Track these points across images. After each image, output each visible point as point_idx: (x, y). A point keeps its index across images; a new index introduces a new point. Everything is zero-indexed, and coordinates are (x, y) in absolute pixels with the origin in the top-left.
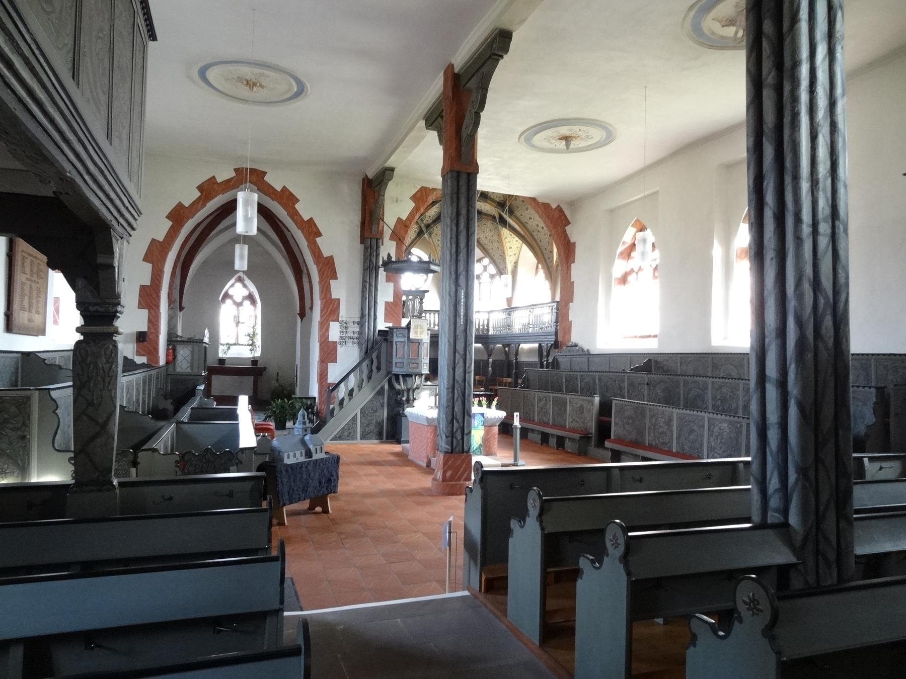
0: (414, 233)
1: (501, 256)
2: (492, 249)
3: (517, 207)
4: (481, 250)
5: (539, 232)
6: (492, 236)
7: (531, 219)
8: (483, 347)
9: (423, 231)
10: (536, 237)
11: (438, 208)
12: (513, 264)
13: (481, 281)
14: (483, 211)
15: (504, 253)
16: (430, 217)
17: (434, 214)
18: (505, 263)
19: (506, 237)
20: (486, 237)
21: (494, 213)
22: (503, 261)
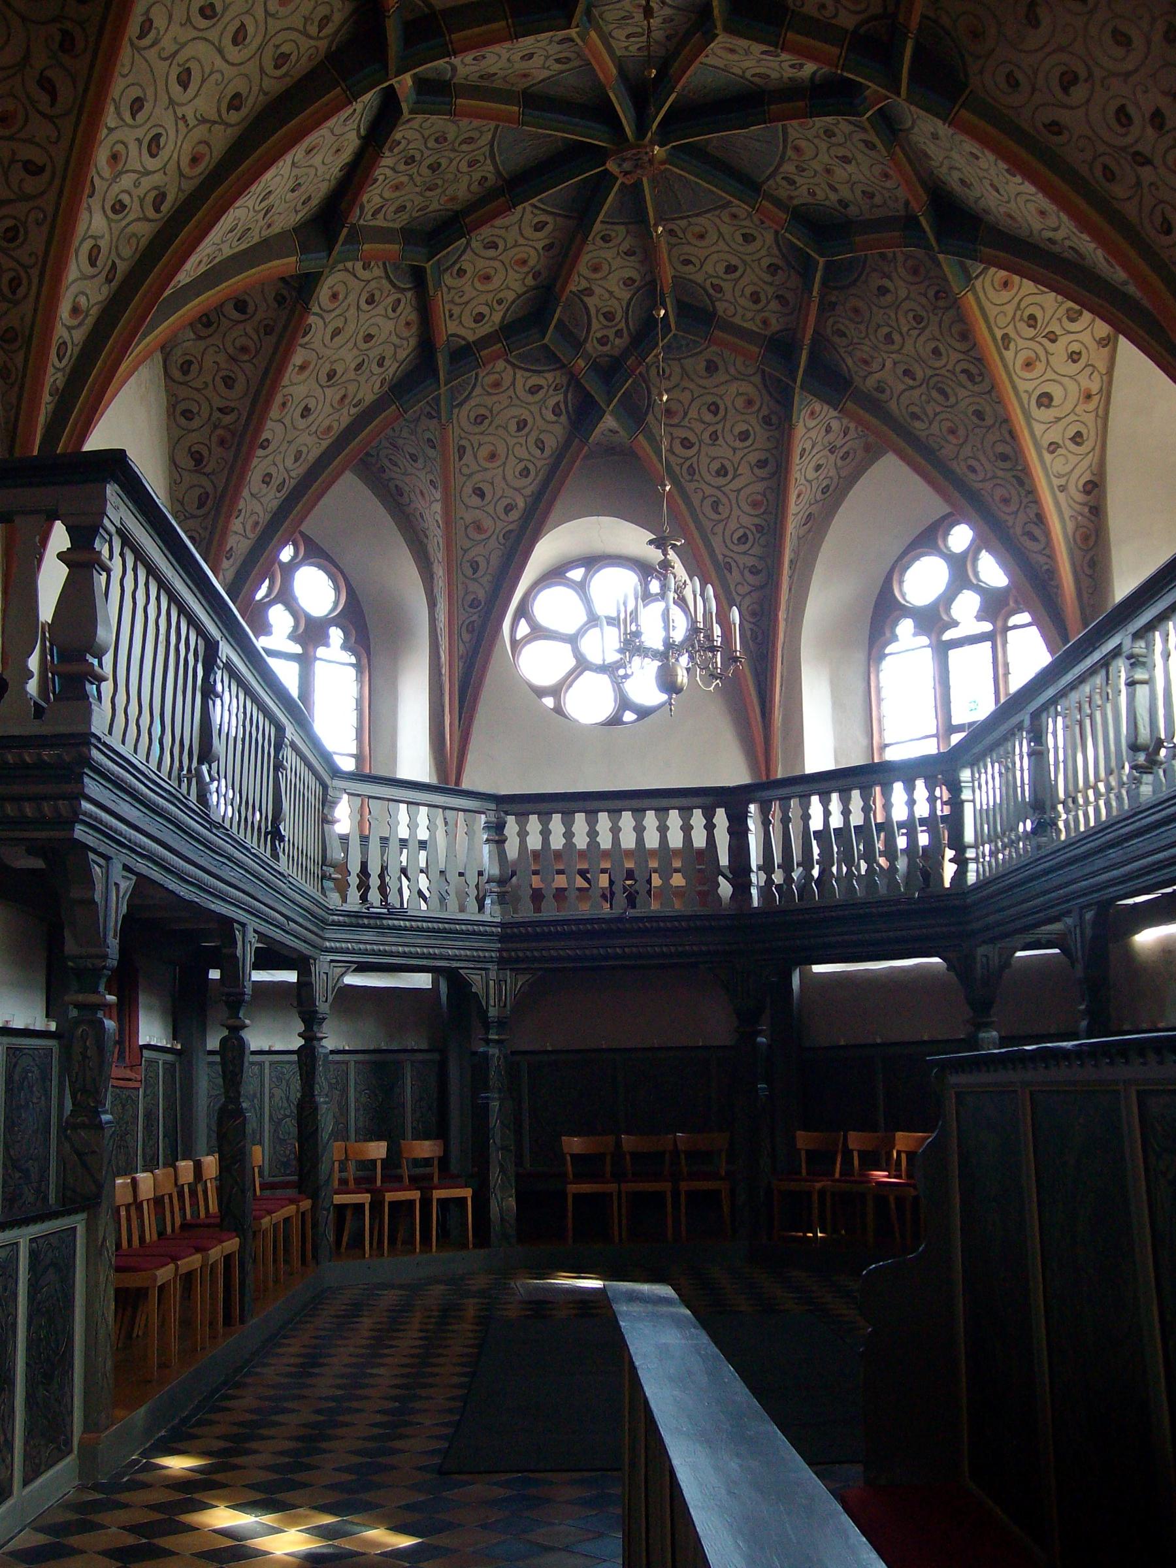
0: (552, 418)
1: (1004, 457)
2: (952, 432)
3: (976, 35)
4: (917, 469)
5: (1141, 159)
6: (936, 352)
7: (1075, 79)
8: (945, 965)
9: (594, 403)
10: (1130, 210)
11: (630, 253)
12: (1080, 497)
13: (948, 635)
14: (853, 211)
15: (1013, 435)
16: (609, 316)
17: (626, 295)
18: (1032, 494)
19: (1005, 337)
20: (906, 373)
21: (902, 193)
22: (1021, 483)
